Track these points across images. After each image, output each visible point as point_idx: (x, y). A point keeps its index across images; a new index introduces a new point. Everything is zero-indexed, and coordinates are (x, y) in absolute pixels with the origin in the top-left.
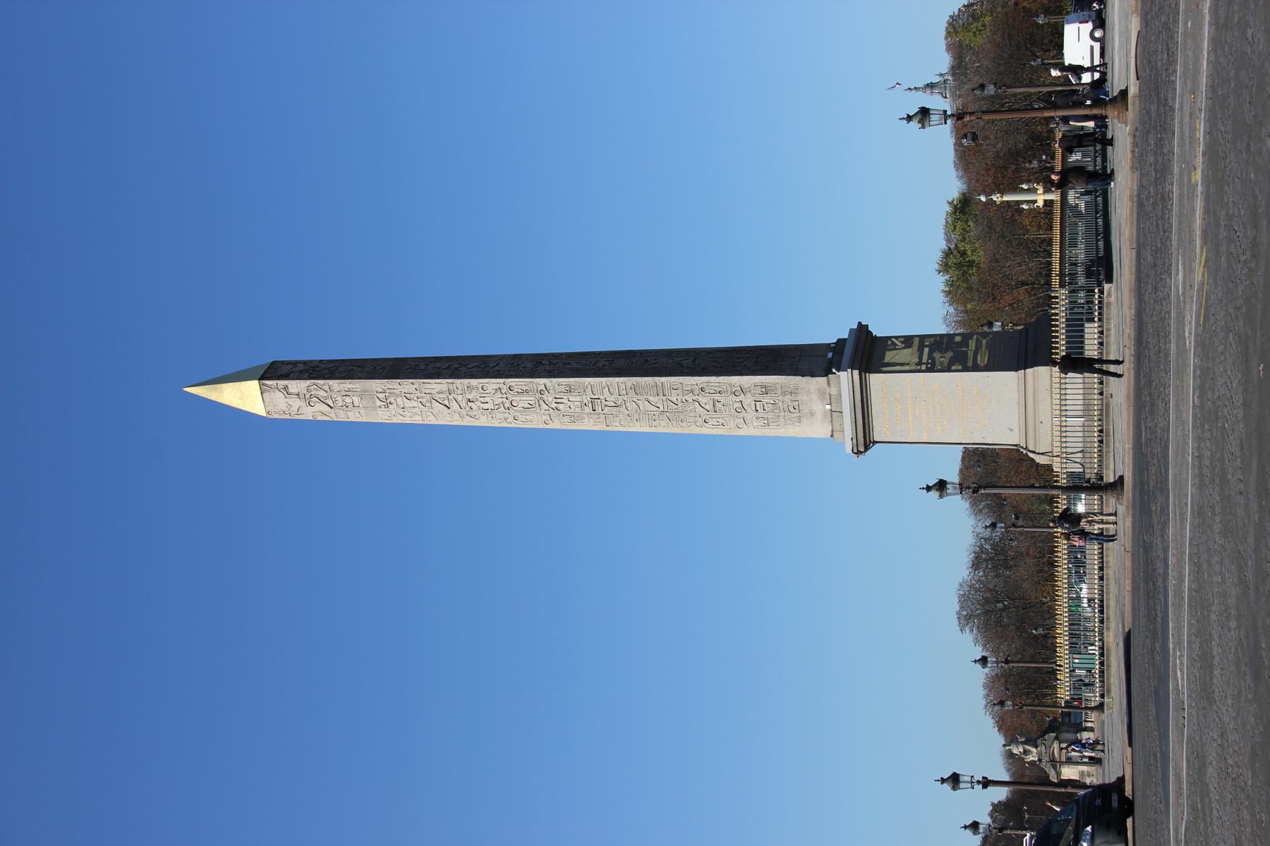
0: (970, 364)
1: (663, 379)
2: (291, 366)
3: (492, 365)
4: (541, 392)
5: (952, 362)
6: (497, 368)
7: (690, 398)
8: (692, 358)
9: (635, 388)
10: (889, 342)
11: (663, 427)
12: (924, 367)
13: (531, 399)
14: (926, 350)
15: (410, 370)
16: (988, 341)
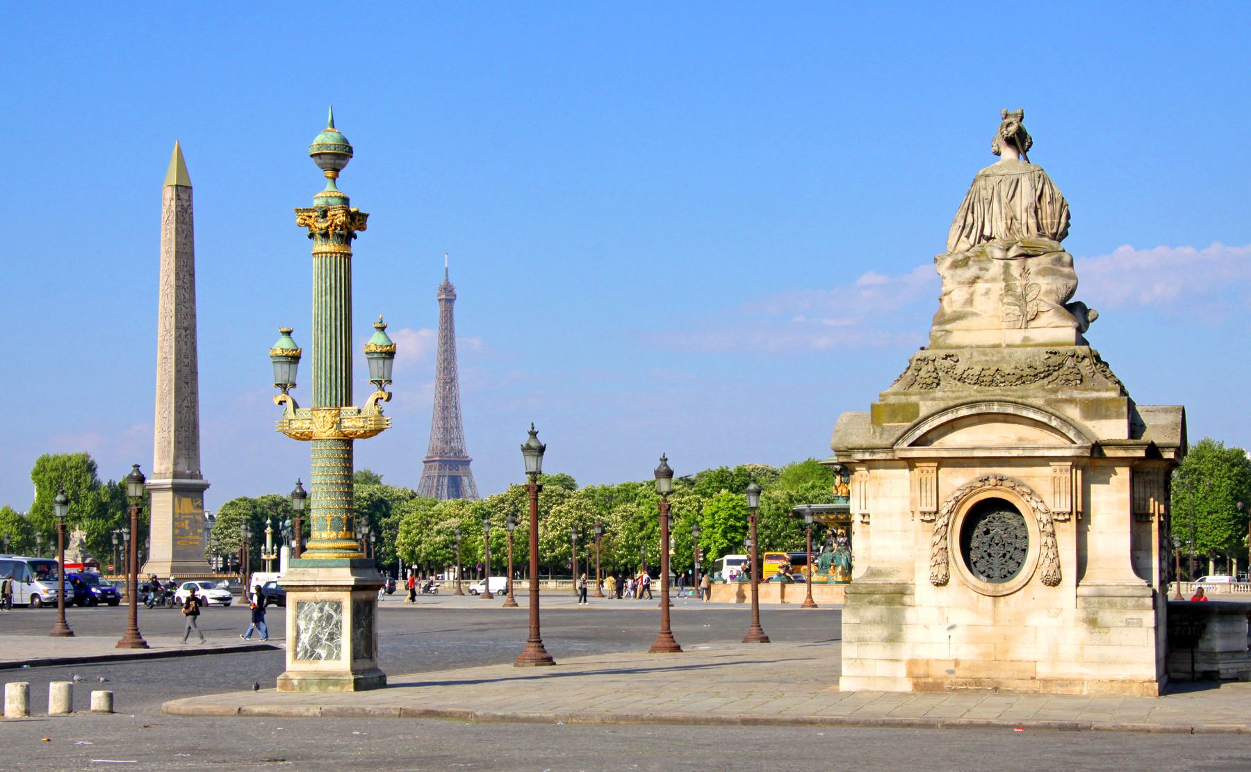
0: (178, 537)
1: (173, 394)
2: (187, 198)
3: (186, 306)
4: (170, 333)
5: (178, 528)
6: (183, 308)
7: (167, 406)
8: (189, 405)
9: (170, 380)
10: (198, 499)
11: (158, 392)
12: (177, 516)
13: (168, 327)
14: (192, 517)
15: (182, 263)
16: (196, 545)
